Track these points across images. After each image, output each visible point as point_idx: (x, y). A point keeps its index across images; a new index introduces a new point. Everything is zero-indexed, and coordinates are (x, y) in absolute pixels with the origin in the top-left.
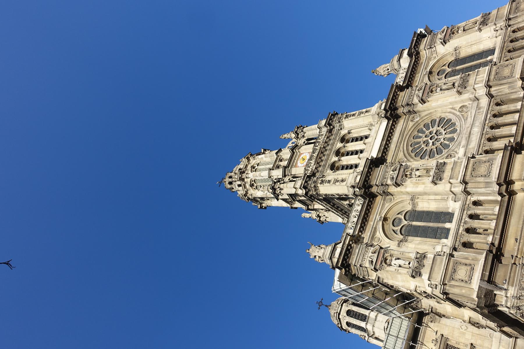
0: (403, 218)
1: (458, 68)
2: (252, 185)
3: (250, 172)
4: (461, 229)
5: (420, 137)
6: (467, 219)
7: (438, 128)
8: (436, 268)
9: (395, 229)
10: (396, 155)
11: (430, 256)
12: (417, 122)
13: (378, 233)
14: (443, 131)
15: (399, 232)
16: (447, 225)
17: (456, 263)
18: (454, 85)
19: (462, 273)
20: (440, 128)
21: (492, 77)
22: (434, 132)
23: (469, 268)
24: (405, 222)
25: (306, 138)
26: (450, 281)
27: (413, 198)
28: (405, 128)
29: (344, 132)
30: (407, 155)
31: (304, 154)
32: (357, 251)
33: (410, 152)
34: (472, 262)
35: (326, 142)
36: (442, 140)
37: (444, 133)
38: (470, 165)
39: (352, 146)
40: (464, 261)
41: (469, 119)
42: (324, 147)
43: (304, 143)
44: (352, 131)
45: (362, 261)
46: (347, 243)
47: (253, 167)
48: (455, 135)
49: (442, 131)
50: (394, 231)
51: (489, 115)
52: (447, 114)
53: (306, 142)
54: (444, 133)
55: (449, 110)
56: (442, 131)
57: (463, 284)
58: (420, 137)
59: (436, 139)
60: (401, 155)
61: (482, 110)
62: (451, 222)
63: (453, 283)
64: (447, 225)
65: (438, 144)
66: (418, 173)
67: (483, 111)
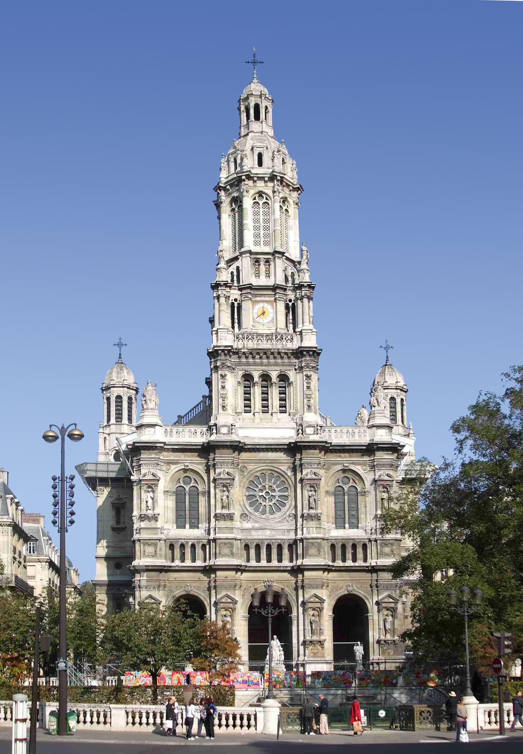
0: (191, 485)
1: (346, 497)
3: (252, 192)
4: (183, 541)
5: (270, 480)
7: (277, 497)
8: (149, 531)
9: (181, 482)
10: (251, 461)
11: (159, 524)
12: (286, 474)
13: (173, 467)
14: (273, 502)
16: (187, 526)
17: (156, 545)
18: (311, 508)
19: (150, 550)
20: (277, 498)
21: (310, 541)
22: (274, 494)
23: (154, 554)
24: (187, 489)
26: (143, 543)
29: (292, 374)
30: (252, 473)
32: (153, 456)
33: (255, 475)
34: (158, 555)
36: (264, 503)
37: (270, 503)
38: (229, 541)
40: (158, 549)
42: (272, 353)
43: (290, 301)
45: (145, 464)
46: (157, 445)
47: (260, 194)
48: (268, 515)
49: (274, 501)
51: (279, 541)
52: (290, 503)
53: (290, 304)
54: (270, 503)
56: (274, 501)
57: (142, 552)
58: (270, 480)
59: (265, 498)
60: (251, 467)
61: (287, 534)
62: (191, 527)
63: (142, 546)
64: (187, 526)
66: (225, 498)
67: (285, 535)
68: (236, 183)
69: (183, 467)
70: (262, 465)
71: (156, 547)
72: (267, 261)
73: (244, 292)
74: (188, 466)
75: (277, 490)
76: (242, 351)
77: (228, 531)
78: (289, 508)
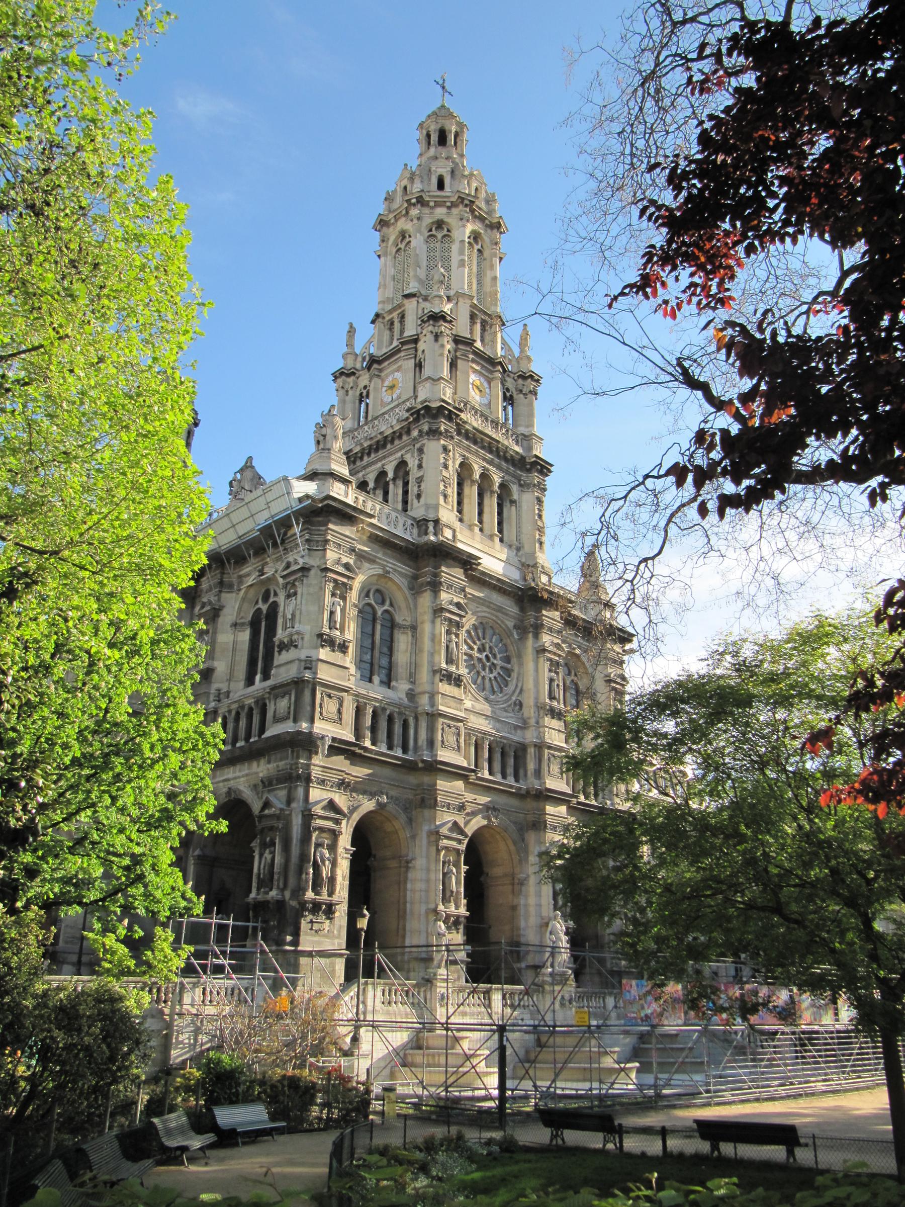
0: (386, 607)
2: (440, 224)
6: (388, 712)
7: (498, 669)
12: (512, 635)
13: (366, 565)
15: (367, 600)
25: (515, 396)
27: (414, 628)
28: (507, 615)
31: (488, 391)
35: (505, 452)
37: (491, 676)
39: (491, 504)
41: (505, 714)
42: (498, 448)
43: (508, 390)
44: (513, 508)
49: (495, 674)
50: (369, 592)
55: (520, 685)
56: (495, 674)
65: (479, 667)
68: (449, 204)
69: (380, 571)
70: (485, 609)
71: (341, 705)
72: (484, 324)
73: (460, 347)
74: (389, 572)
75: (498, 656)
76: (467, 427)
77: (453, 704)
78: (514, 692)
